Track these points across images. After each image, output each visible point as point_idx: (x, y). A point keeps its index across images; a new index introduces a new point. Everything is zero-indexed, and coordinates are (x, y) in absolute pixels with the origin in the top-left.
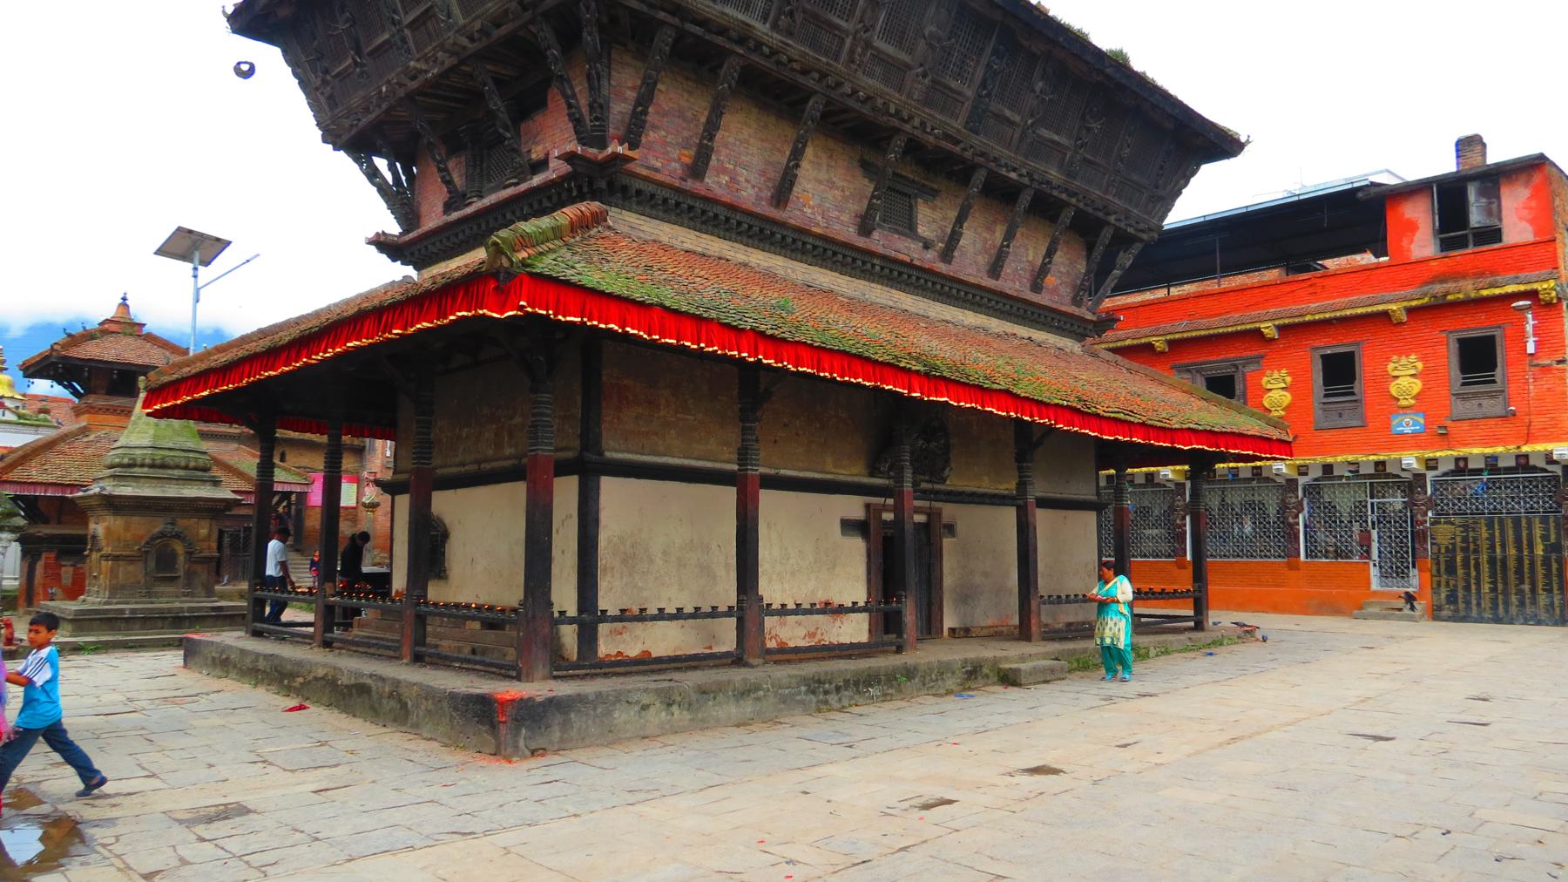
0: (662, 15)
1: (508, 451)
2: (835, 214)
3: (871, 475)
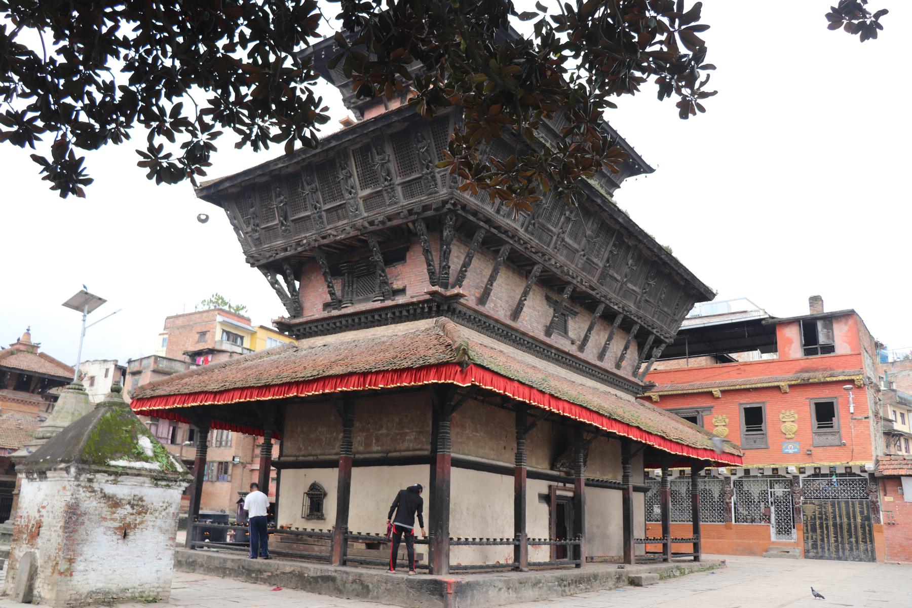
0: (482, 224)
1: (375, 448)
2: (535, 325)
3: (552, 469)
